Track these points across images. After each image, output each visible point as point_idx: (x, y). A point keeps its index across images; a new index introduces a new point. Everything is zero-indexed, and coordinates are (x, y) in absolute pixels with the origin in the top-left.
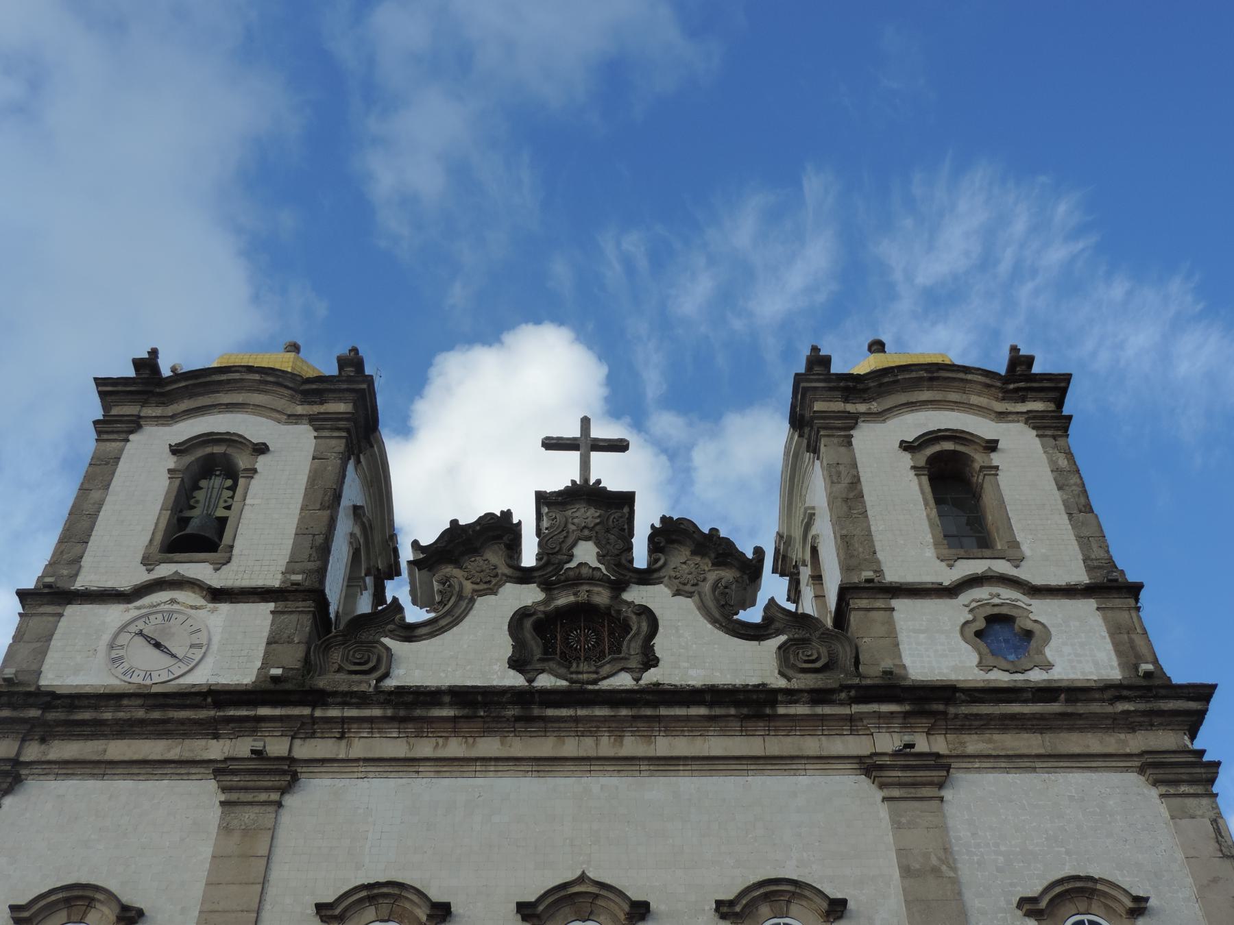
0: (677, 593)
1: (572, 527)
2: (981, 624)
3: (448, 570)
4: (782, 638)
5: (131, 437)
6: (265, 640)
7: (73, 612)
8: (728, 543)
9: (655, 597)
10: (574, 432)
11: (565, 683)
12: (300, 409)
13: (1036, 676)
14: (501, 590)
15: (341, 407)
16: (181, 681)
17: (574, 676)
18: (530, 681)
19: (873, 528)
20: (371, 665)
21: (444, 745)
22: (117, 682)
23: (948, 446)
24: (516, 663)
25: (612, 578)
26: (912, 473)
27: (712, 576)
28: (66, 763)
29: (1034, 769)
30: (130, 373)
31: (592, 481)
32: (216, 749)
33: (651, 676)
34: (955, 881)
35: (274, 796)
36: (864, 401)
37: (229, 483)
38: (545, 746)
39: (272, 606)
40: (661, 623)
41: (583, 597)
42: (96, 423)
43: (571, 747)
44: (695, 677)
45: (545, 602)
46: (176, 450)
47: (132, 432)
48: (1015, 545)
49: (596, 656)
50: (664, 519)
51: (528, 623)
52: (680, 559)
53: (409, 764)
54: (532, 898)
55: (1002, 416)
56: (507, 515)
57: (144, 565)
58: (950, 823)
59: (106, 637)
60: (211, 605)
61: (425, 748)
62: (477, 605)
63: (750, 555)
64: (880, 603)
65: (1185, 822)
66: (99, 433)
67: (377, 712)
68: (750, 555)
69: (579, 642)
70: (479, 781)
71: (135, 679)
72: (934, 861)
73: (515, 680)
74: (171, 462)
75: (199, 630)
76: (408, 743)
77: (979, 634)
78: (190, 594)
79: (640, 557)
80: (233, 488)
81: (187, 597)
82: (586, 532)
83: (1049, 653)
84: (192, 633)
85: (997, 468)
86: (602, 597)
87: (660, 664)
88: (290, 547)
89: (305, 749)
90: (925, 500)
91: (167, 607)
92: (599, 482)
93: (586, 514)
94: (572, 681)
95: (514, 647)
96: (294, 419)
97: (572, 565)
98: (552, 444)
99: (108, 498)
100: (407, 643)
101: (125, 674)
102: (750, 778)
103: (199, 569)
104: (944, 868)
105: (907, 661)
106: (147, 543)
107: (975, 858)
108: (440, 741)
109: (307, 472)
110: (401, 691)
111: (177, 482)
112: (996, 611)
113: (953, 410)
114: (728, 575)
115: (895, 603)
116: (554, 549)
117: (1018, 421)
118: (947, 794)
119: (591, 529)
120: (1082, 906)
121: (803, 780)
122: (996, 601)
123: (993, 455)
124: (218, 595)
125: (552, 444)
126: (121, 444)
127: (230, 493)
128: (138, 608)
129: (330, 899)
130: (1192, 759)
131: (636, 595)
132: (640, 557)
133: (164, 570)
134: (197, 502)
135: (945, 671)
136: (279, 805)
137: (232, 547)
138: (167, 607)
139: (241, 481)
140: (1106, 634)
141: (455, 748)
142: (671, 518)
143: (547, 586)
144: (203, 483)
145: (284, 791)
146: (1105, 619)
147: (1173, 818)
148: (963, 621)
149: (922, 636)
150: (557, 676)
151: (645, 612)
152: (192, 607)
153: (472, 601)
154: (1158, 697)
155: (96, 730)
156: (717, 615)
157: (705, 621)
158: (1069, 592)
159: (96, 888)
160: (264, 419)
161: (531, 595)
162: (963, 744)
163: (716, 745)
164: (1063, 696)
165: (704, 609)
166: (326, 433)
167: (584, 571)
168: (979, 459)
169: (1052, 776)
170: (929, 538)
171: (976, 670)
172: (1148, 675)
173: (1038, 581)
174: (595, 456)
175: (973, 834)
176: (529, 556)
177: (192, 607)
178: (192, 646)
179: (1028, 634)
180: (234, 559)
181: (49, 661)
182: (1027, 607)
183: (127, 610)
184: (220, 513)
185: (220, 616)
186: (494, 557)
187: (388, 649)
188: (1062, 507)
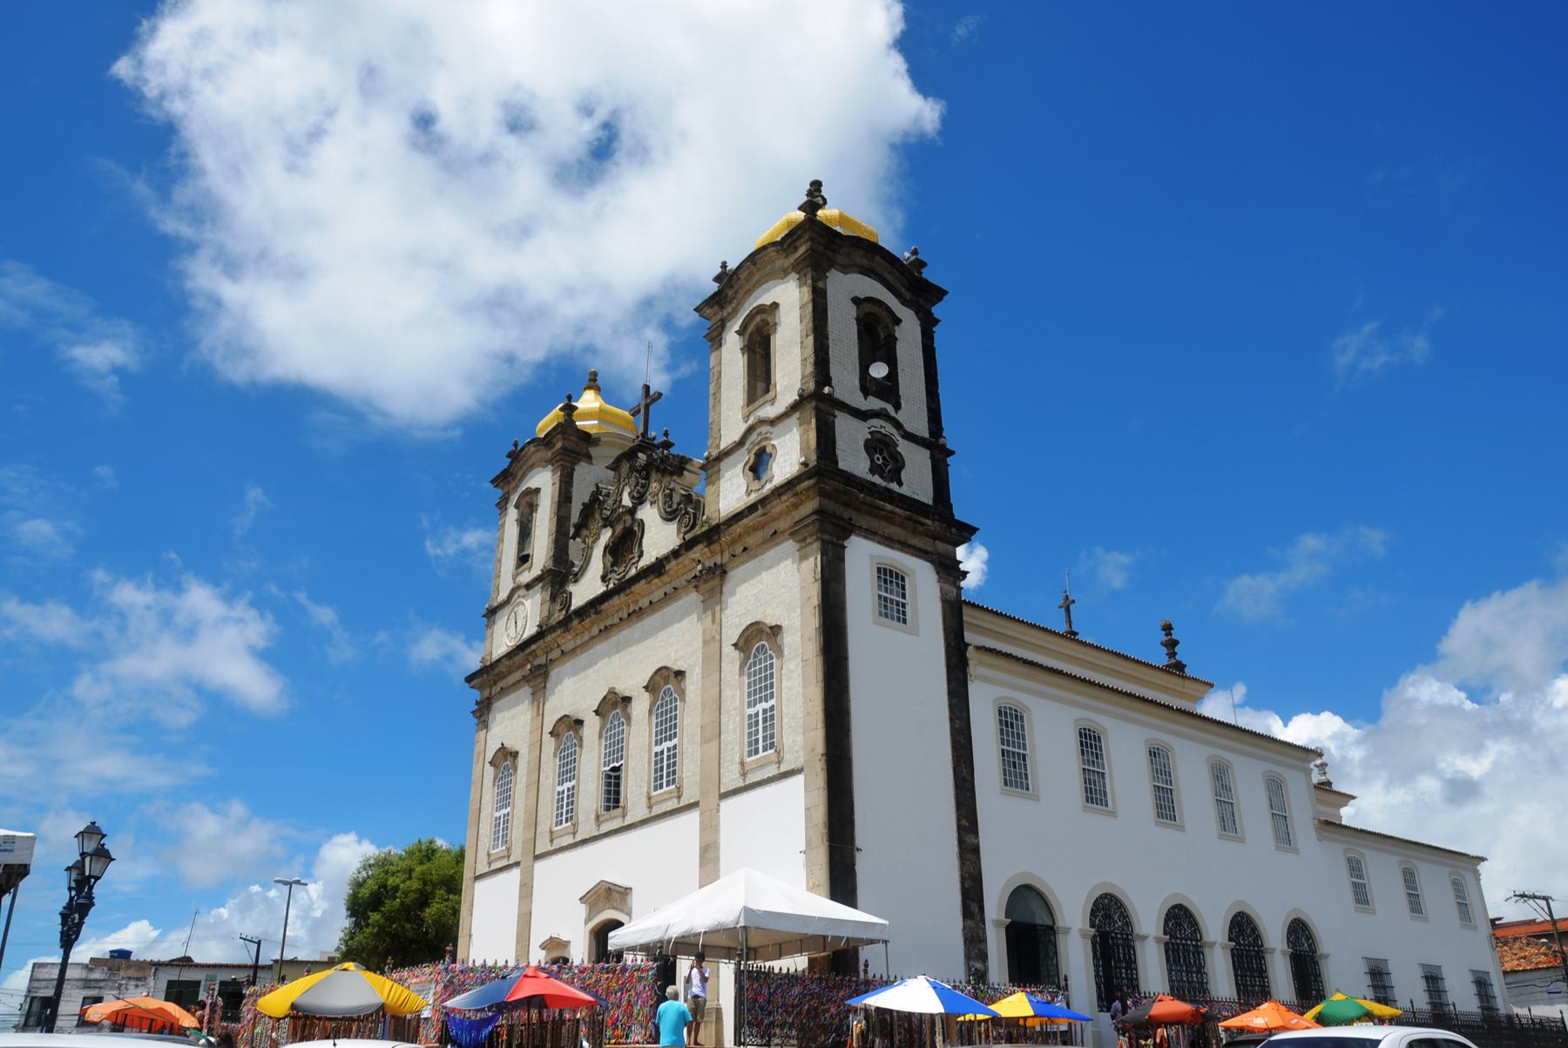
39: (540, 585)
120: (758, 639)
151: (641, 524)
154: (795, 486)
164: (760, 507)
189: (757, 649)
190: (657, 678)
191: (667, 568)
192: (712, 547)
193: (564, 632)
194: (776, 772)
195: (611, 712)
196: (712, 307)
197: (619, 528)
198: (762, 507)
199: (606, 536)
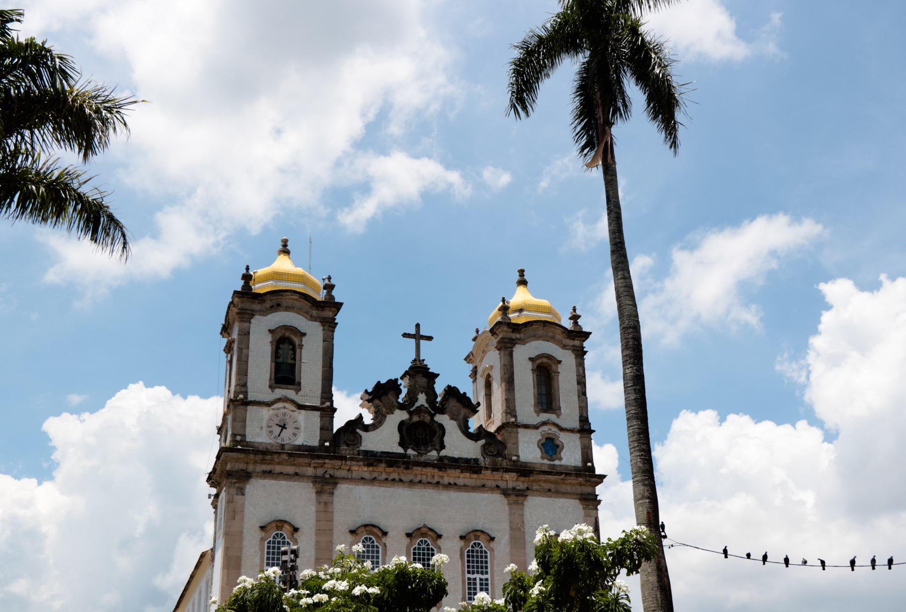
0: (452, 419)
1: (417, 386)
2: (544, 441)
3: (377, 401)
4: (483, 442)
5: (252, 321)
6: (319, 428)
7: (250, 408)
8: (469, 399)
9: (443, 419)
10: (413, 332)
11: (416, 453)
12: (315, 313)
13: (557, 462)
14: (395, 412)
17: (419, 451)
18: (406, 451)
19: (516, 396)
20: (354, 443)
21: (381, 475)
23: (545, 360)
24: (402, 444)
25: (432, 412)
26: (531, 372)
29: (551, 497)
30: (243, 281)
31: (421, 358)
32: (310, 471)
33: (443, 453)
34: (524, 532)
36: (519, 333)
37: (291, 347)
39: (319, 412)
40: (446, 431)
44: (456, 454)
45: (410, 419)
47: (252, 318)
48: (560, 408)
51: (404, 428)
52: (453, 404)
55: (564, 347)
57: (271, 389)
58: (525, 513)
60: (298, 410)
62: (387, 418)
64: (514, 430)
65: (588, 518)
69: (419, 435)
70: (392, 489)
72: (519, 526)
73: (400, 450)
74: (269, 338)
75: (296, 421)
76: (370, 473)
77: (542, 444)
78: (290, 404)
80: (294, 350)
81: (288, 405)
82: (422, 389)
83: (562, 454)
84: (294, 422)
85: (559, 372)
86: (427, 418)
87: (446, 448)
88: (321, 385)
90: (534, 384)
92: (424, 360)
93: (422, 381)
94: (418, 453)
95: (400, 437)
96: (313, 318)
97: (417, 404)
98: (406, 335)
99: (250, 353)
100: (365, 433)
101: (274, 438)
102: (471, 493)
103: (290, 393)
104: (522, 528)
105: (520, 454)
106: (269, 378)
107: (530, 525)
108: (380, 473)
109: (322, 348)
110: (366, 453)
111: (274, 347)
112: (549, 436)
113: (548, 341)
115: (520, 430)
117: (570, 349)
119: (424, 388)
121: (486, 495)
122: (550, 432)
123: (559, 366)
124: (301, 407)
125: (406, 335)
126: (248, 324)
127: (291, 352)
128: (273, 409)
130: (594, 497)
131: (439, 418)
133: (280, 392)
134: (280, 355)
135: (531, 458)
136: (332, 493)
137: (300, 383)
138: (283, 411)
139: (298, 351)
140: (580, 448)
142: (451, 386)
143: (411, 414)
144: (281, 346)
145: (333, 489)
146: (581, 443)
147: (585, 516)
148: (539, 439)
149: (526, 444)
150: (414, 450)
151: (441, 427)
152: (292, 411)
153: (386, 417)
156: (464, 429)
157: (460, 432)
158: (572, 431)
159: (286, 522)
160: (302, 317)
162: (532, 486)
167: (423, 408)
168: (554, 367)
169: (555, 499)
170: (533, 402)
171: (540, 459)
172: (589, 467)
173: (564, 425)
174: (422, 341)
175: (531, 517)
177: (292, 411)
178: (296, 428)
179: (557, 446)
180: (302, 389)
182: (559, 436)
183: (269, 410)
184: (290, 361)
185: (302, 415)
186: (391, 397)
187: (361, 436)
188: (577, 393)
190: (472, 534)
191: (483, 472)
192: (520, 478)
193: (364, 465)
195: (419, 538)
196: (509, 328)
197: (416, 419)
198: (565, 476)
199: (400, 416)
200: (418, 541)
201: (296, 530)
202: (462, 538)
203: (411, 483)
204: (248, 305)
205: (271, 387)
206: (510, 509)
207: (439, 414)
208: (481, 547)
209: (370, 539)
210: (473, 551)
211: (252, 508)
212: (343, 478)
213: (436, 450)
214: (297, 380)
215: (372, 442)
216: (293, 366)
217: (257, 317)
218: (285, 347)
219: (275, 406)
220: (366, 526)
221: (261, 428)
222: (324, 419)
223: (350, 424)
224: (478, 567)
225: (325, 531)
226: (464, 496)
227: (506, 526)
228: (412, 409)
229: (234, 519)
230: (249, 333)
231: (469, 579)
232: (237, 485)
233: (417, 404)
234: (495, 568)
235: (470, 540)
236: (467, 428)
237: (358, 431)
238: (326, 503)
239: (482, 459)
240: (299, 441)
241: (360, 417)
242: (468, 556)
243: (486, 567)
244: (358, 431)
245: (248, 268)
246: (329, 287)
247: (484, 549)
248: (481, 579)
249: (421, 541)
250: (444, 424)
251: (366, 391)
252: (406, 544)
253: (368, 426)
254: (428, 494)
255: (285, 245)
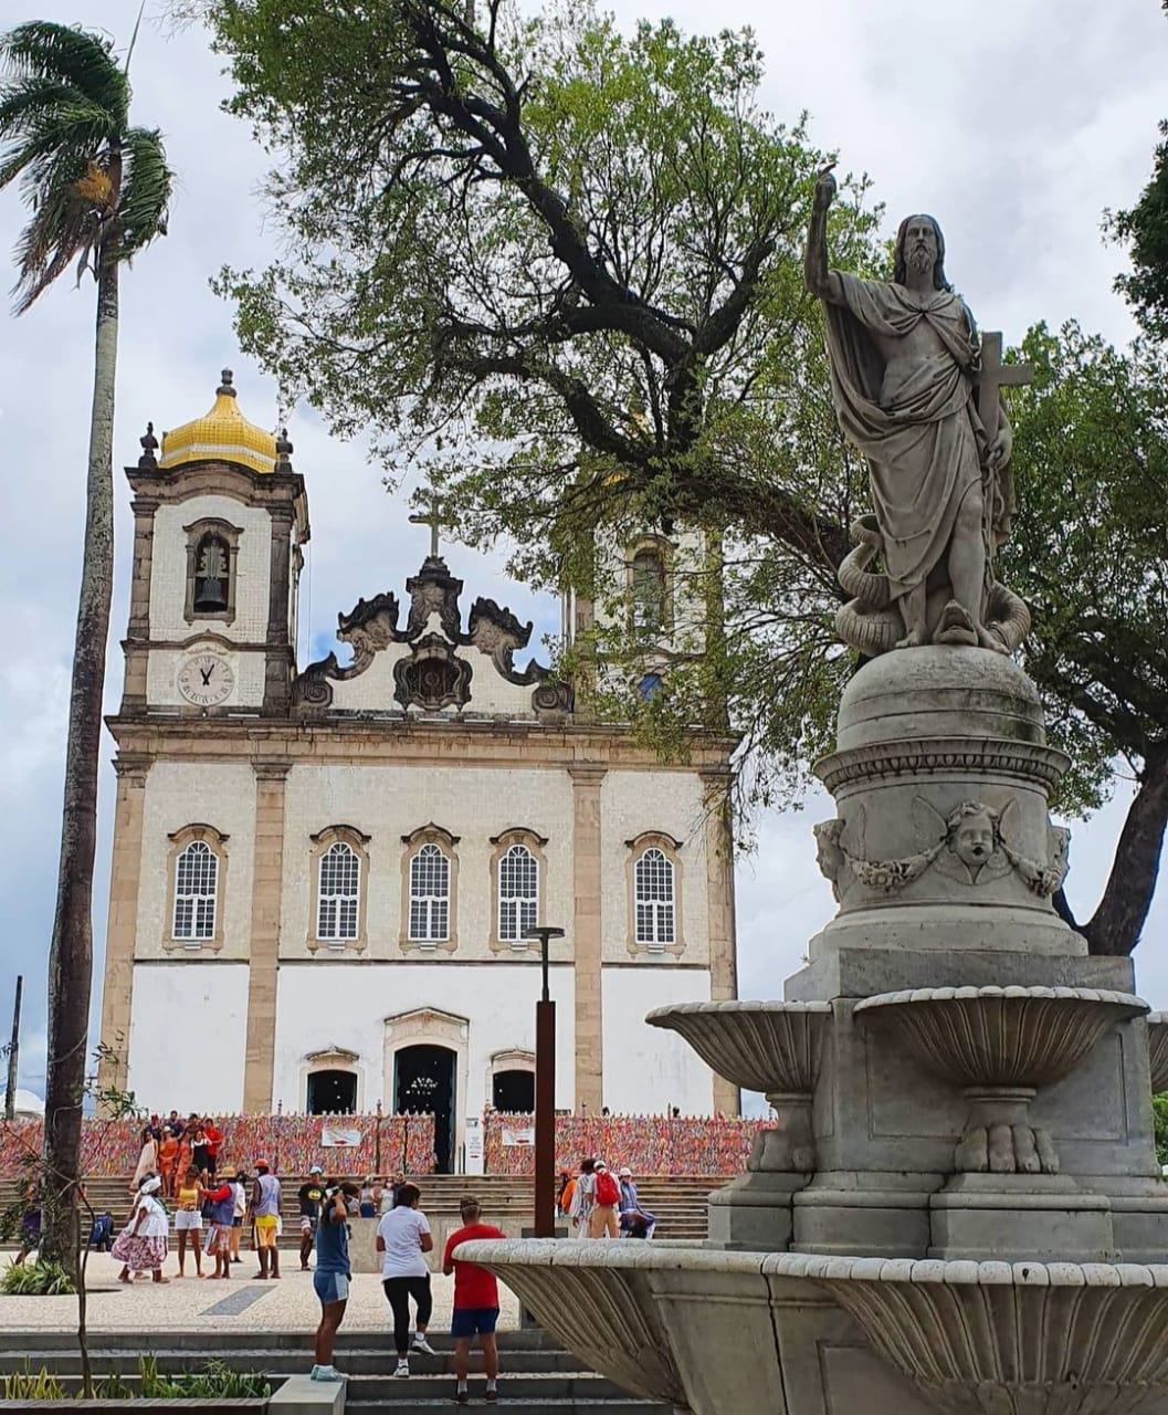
0: (484, 652)
3: (358, 632)
4: (537, 685)
7: (152, 653)
12: (258, 494)
15: (282, 494)
16: (223, 704)
22: (186, 703)
25: (450, 642)
27: (503, 641)
28: (174, 754)
32: (248, 747)
35: (282, 775)
37: (222, 551)
38: (412, 750)
41: (433, 654)
42: (132, 504)
43: (426, 751)
46: (188, 529)
49: (439, 694)
50: (479, 599)
52: (485, 626)
53: (349, 758)
54: (408, 834)
56: (391, 594)
59: (177, 672)
61: (354, 750)
63: (525, 626)
66: (134, 510)
67: (329, 731)
68: (525, 626)
71: (200, 702)
74: (185, 539)
79: (465, 630)
80: (226, 556)
86: (443, 655)
89: (295, 749)
91: (206, 653)
93: (434, 593)
97: (426, 632)
103: (217, 626)
114: (511, 639)
116: (417, 623)
118: (603, 782)
121: (538, 772)
124: (233, 646)
128: (191, 653)
129: (317, 833)
131: (462, 652)
132: (465, 630)
133: (200, 626)
136: (284, 779)
138: (206, 653)
139: (232, 556)
141: (369, 750)
143: (415, 648)
145: (286, 771)
150: (421, 706)
151: (466, 666)
155: (184, 735)
161: (401, 651)
162: (618, 754)
163: (497, 752)
165: (496, 663)
166: (277, 517)
167: (434, 637)
176: (402, 626)
181: (150, 686)
184: (224, 575)
185: (236, 660)
189: (651, 852)
194: (675, 961)
197: (423, 655)
200: (423, 847)
201: (224, 838)
202: (494, 841)
203: (412, 760)
204: (152, 490)
205: (186, 618)
206: (577, 794)
207: (463, 644)
208: (527, 854)
209: (344, 846)
210: (511, 861)
211: (156, 807)
212: (303, 756)
213: (456, 703)
214: (230, 604)
215: (347, 695)
216: (225, 583)
217: (164, 507)
218: (213, 553)
219: (193, 648)
220: (335, 828)
221: (171, 685)
222: (272, 663)
223: (313, 669)
224: (518, 886)
225: (269, 838)
226: (499, 775)
227: (569, 819)
228: (416, 641)
229: (128, 824)
230: (152, 533)
231: (504, 904)
232: (132, 773)
233: (426, 632)
234: (548, 887)
235: (507, 842)
236: (509, 664)
237: (328, 679)
238: (272, 794)
239: (534, 713)
240: (233, 701)
241: (332, 657)
242: (504, 869)
243: (534, 886)
244: (328, 679)
245: (150, 428)
246: (285, 448)
247: (530, 857)
248: (523, 904)
249: (427, 848)
250: (469, 661)
251: (341, 615)
252: (401, 853)
253: (344, 670)
254: (441, 773)
255: (227, 382)
